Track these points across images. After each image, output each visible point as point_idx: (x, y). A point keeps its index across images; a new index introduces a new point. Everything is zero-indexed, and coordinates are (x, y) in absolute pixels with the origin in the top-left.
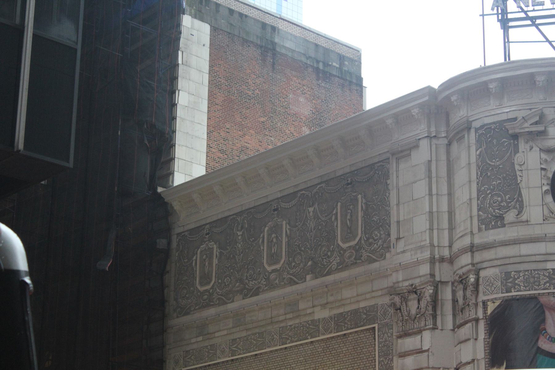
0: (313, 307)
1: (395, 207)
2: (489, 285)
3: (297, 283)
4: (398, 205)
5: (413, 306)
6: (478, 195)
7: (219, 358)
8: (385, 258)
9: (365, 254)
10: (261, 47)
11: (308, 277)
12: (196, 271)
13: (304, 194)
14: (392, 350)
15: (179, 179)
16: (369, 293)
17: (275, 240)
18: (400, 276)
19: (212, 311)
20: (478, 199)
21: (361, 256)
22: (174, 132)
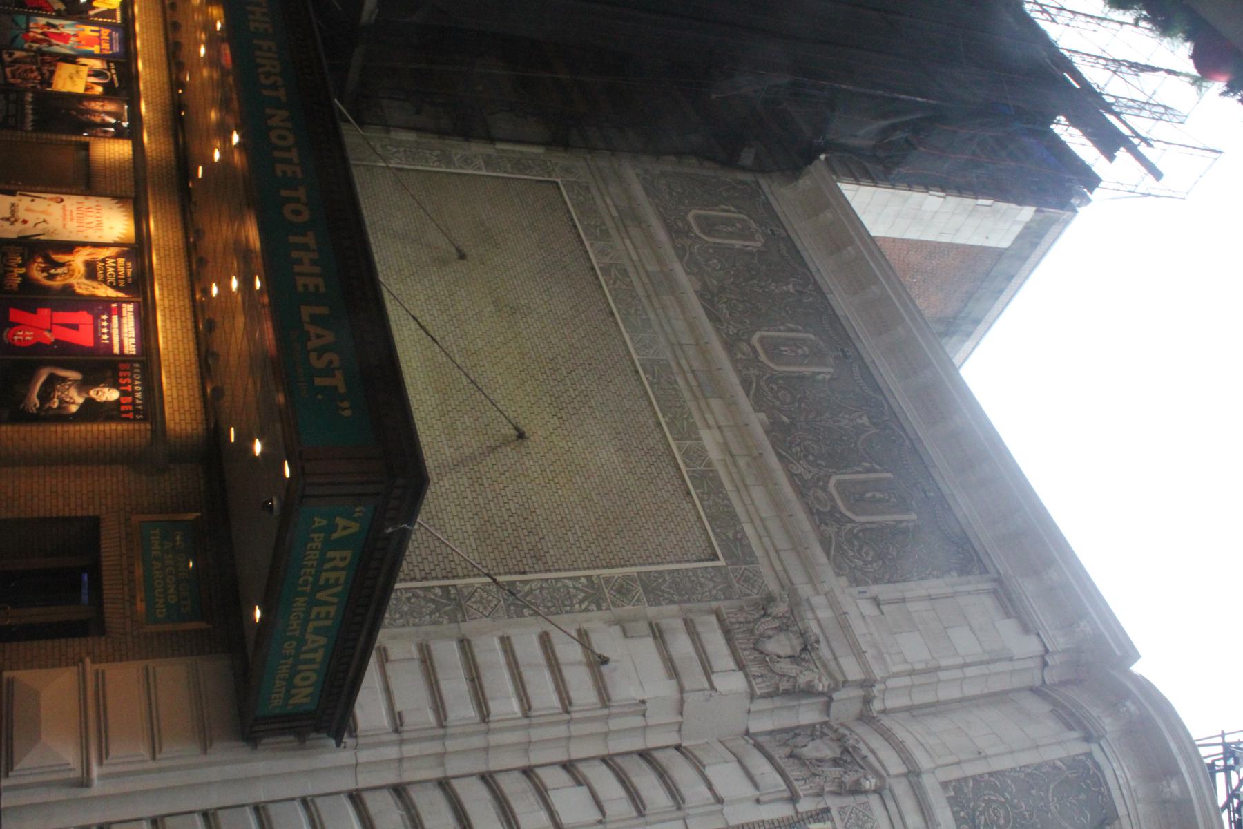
0: (719, 427)
1: (924, 592)
2: (858, 819)
3: (748, 395)
4: (930, 598)
5: (780, 645)
6: (995, 773)
7: (592, 245)
8: (838, 575)
9: (831, 530)
10: (955, 318)
11: (763, 416)
14: (689, 601)
16: (773, 544)
17: (800, 351)
18: (824, 614)
19: (661, 235)
20: (990, 774)
21: (826, 524)
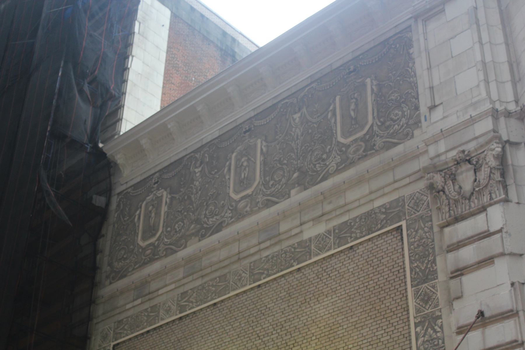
1: (425, 73)
3: (277, 203)
4: (429, 68)
5: (466, 179)
7: (163, 319)
8: (412, 136)
9: (379, 142)
10: (221, 50)
11: (293, 192)
12: (138, 226)
13: (287, 103)
14: (433, 248)
15: (125, 127)
16: (389, 185)
17: (245, 164)
18: (442, 147)
19: (156, 266)
21: (374, 145)
22: (124, 93)
